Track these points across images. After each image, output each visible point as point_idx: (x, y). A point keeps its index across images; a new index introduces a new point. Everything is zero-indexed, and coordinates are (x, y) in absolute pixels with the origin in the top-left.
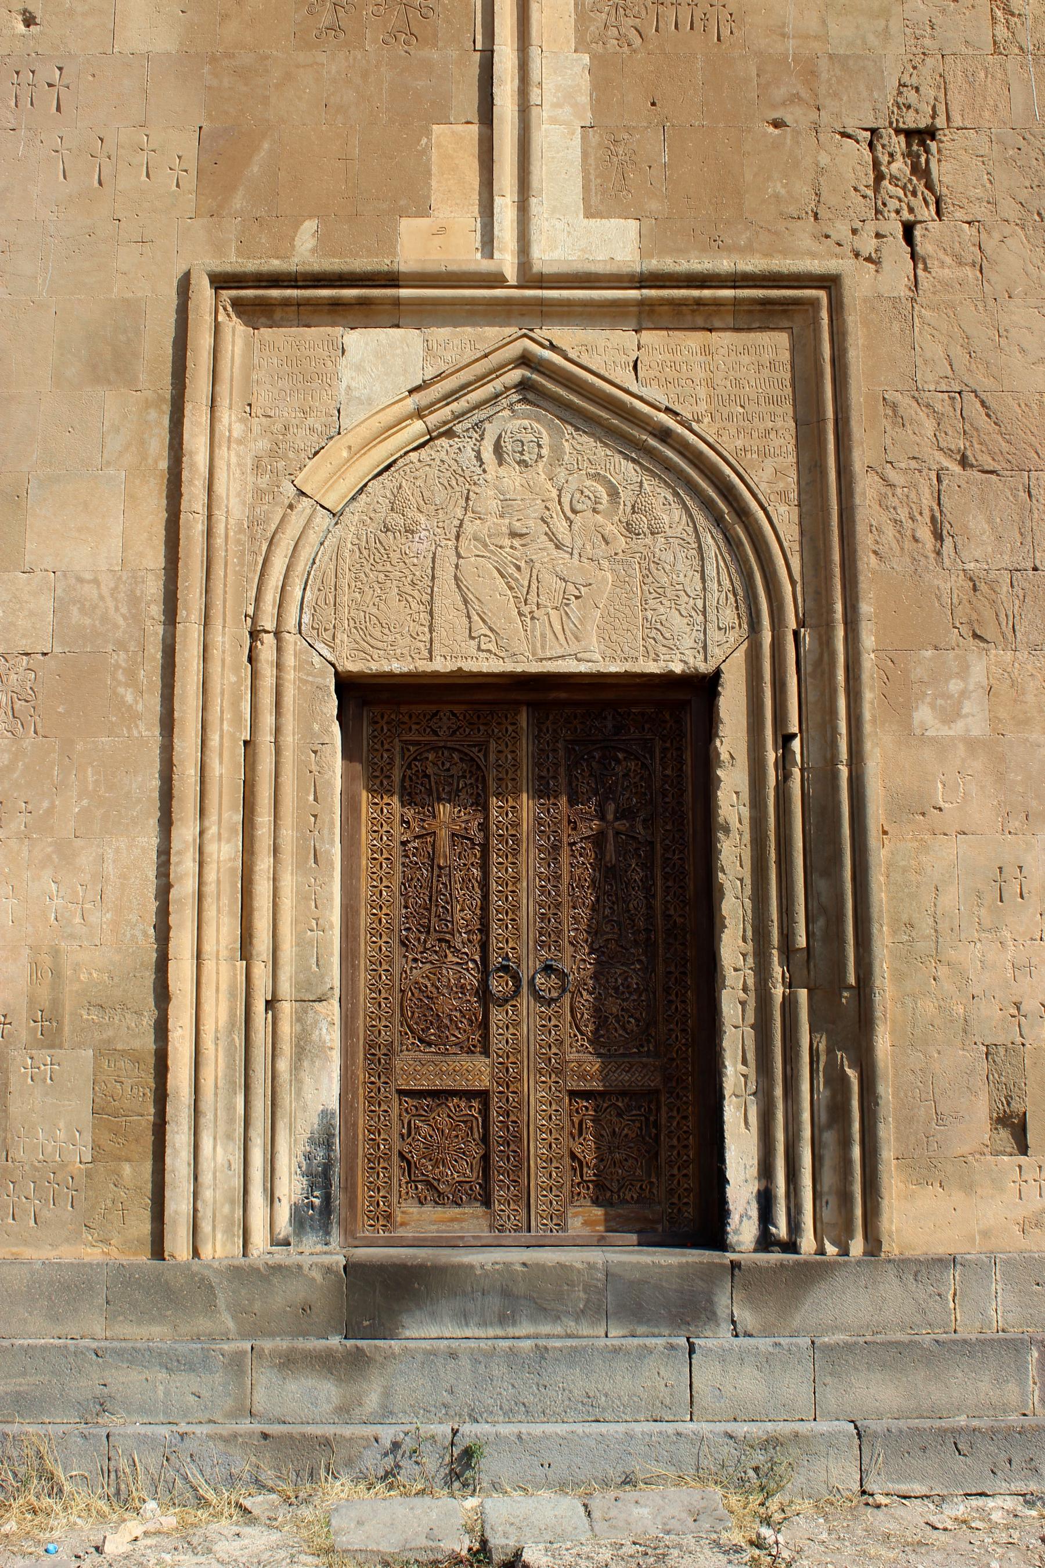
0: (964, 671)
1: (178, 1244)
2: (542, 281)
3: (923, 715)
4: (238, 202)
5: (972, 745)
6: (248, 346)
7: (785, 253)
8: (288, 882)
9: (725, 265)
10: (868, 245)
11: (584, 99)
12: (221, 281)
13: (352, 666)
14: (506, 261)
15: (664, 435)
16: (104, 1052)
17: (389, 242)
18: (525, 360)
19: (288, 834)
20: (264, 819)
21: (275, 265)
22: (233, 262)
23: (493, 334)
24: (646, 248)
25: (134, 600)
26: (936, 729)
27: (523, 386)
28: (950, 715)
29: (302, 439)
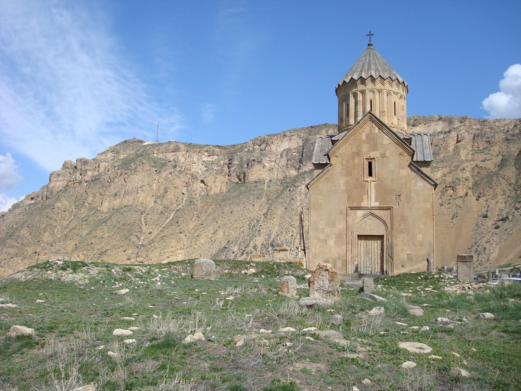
0: (401, 235)
1: (348, 272)
2: (372, 207)
3: (398, 238)
4: (350, 201)
5: (401, 240)
6: (351, 212)
7: (389, 205)
8: (354, 249)
9: (385, 206)
10: (395, 204)
11: (375, 193)
12: (349, 207)
13: (359, 234)
14: (369, 206)
15: (380, 218)
16: (343, 260)
17: (361, 205)
18: (370, 213)
19: (354, 246)
20: (353, 245)
21: (353, 206)
22: (350, 206)
23: (368, 211)
24: (379, 204)
25: (344, 230)
26: (398, 239)
27: (370, 214)
28: (400, 238)
29: (355, 218)
